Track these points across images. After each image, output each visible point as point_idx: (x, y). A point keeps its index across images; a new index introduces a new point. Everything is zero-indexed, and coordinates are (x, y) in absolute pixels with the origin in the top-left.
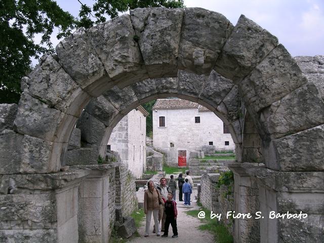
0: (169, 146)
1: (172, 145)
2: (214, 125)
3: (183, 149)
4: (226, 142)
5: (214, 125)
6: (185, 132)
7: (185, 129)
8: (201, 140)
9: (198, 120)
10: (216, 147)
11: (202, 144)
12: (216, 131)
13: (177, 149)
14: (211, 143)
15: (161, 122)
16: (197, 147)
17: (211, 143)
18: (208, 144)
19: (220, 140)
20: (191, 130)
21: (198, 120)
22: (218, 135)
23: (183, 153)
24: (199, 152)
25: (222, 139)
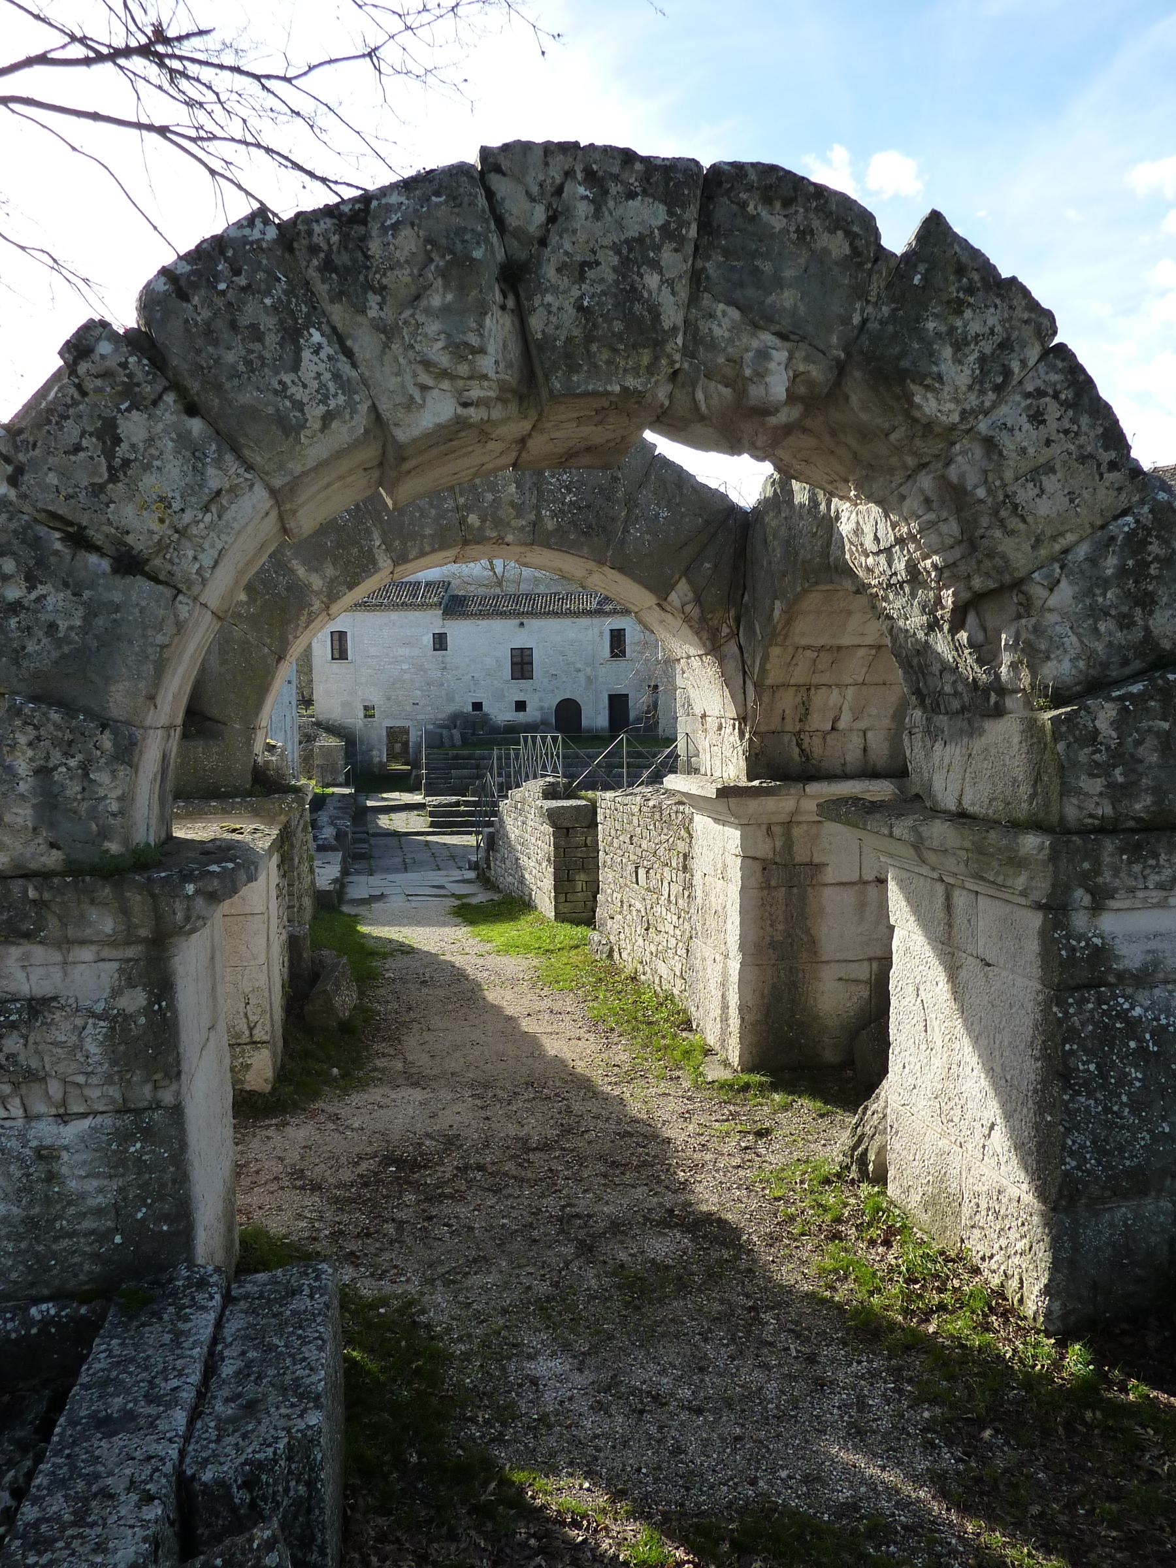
0: (361, 714)
1: (369, 711)
3: (399, 723)
4: (517, 702)
6: (407, 676)
7: (405, 667)
8: (450, 698)
9: (440, 642)
11: (451, 708)
13: (383, 723)
14: (477, 706)
15: (336, 643)
16: (440, 716)
17: (477, 706)
18: (470, 708)
20: (421, 668)
21: (440, 642)
23: (396, 735)
24: (445, 732)
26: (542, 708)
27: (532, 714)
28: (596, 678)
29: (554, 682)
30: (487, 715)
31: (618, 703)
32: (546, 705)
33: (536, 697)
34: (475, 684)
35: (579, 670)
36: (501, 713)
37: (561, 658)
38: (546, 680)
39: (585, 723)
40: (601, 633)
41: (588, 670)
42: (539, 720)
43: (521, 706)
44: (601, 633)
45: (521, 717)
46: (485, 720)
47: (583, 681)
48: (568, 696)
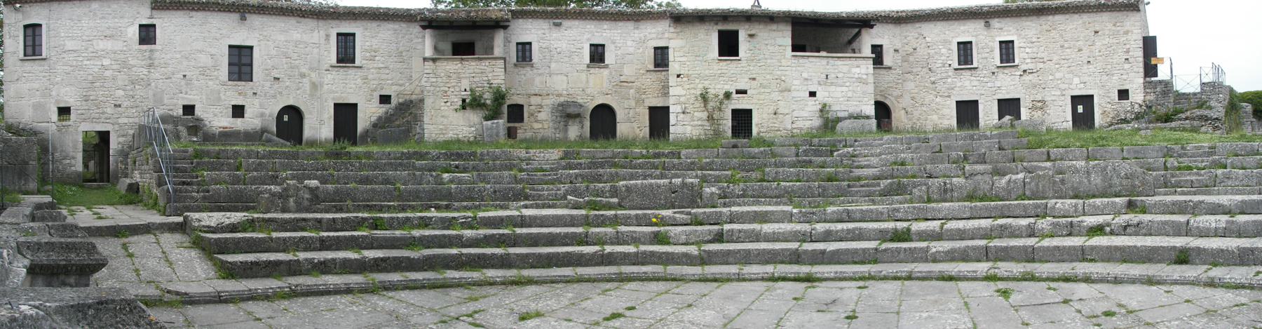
2: (200, 52)
4: (234, 107)
5: (200, 52)
10: (207, 123)
12: (204, 71)
14: (189, 109)
17: (189, 109)
19: (219, 99)
22: (211, 83)
25: (223, 97)
26: (262, 115)
27: (250, 122)
28: (322, 86)
29: (276, 86)
30: (199, 120)
31: (345, 114)
32: (267, 112)
33: (256, 101)
34: (187, 84)
35: (303, 76)
36: (217, 119)
37: (284, 60)
38: (268, 84)
39: (308, 133)
40: (328, 36)
41: (313, 75)
42: (258, 128)
43: (238, 111)
44: (328, 36)
45: (239, 124)
46: (196, 128)
47: (307, 87)
48: (291, 102)
